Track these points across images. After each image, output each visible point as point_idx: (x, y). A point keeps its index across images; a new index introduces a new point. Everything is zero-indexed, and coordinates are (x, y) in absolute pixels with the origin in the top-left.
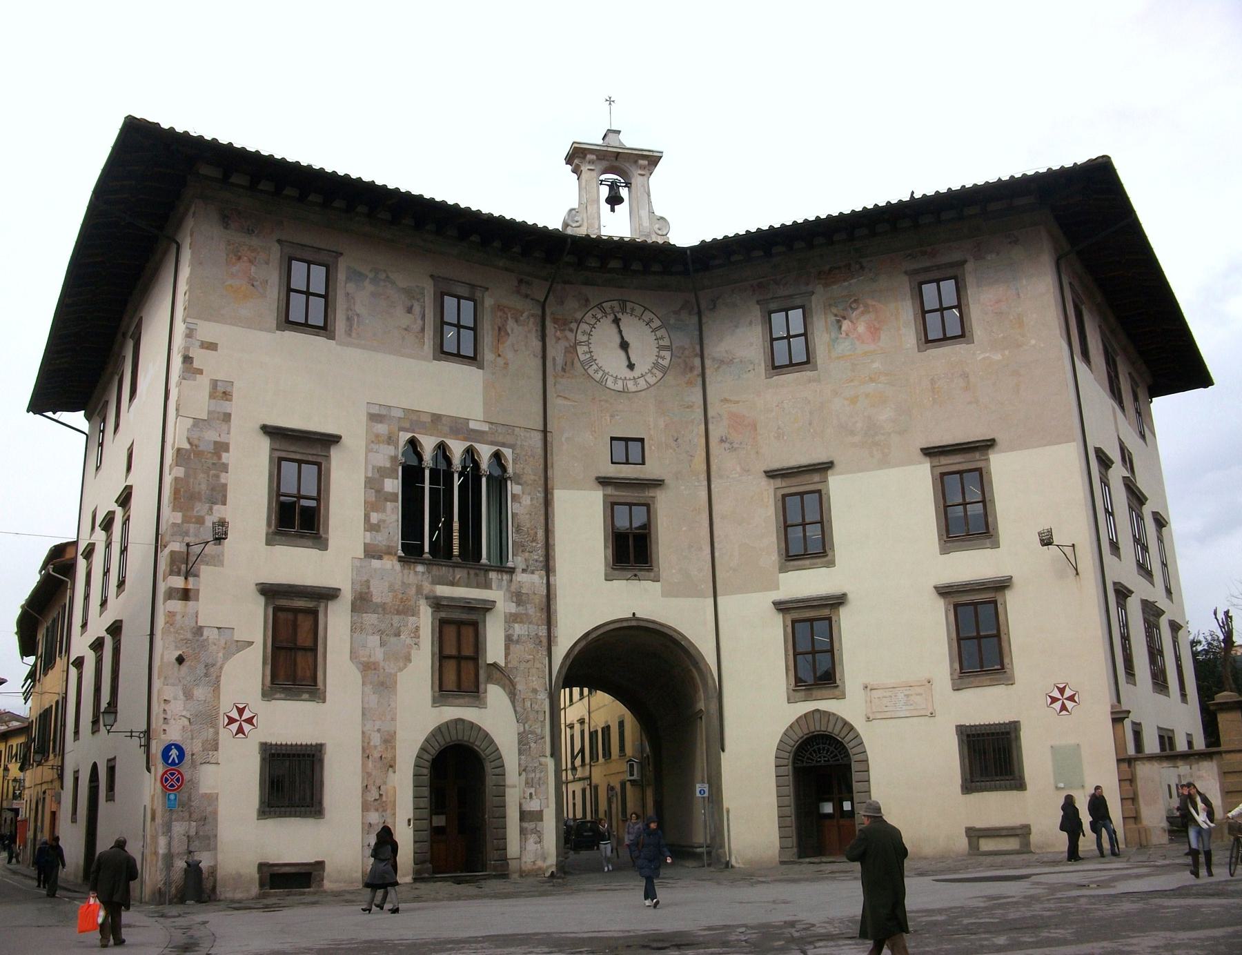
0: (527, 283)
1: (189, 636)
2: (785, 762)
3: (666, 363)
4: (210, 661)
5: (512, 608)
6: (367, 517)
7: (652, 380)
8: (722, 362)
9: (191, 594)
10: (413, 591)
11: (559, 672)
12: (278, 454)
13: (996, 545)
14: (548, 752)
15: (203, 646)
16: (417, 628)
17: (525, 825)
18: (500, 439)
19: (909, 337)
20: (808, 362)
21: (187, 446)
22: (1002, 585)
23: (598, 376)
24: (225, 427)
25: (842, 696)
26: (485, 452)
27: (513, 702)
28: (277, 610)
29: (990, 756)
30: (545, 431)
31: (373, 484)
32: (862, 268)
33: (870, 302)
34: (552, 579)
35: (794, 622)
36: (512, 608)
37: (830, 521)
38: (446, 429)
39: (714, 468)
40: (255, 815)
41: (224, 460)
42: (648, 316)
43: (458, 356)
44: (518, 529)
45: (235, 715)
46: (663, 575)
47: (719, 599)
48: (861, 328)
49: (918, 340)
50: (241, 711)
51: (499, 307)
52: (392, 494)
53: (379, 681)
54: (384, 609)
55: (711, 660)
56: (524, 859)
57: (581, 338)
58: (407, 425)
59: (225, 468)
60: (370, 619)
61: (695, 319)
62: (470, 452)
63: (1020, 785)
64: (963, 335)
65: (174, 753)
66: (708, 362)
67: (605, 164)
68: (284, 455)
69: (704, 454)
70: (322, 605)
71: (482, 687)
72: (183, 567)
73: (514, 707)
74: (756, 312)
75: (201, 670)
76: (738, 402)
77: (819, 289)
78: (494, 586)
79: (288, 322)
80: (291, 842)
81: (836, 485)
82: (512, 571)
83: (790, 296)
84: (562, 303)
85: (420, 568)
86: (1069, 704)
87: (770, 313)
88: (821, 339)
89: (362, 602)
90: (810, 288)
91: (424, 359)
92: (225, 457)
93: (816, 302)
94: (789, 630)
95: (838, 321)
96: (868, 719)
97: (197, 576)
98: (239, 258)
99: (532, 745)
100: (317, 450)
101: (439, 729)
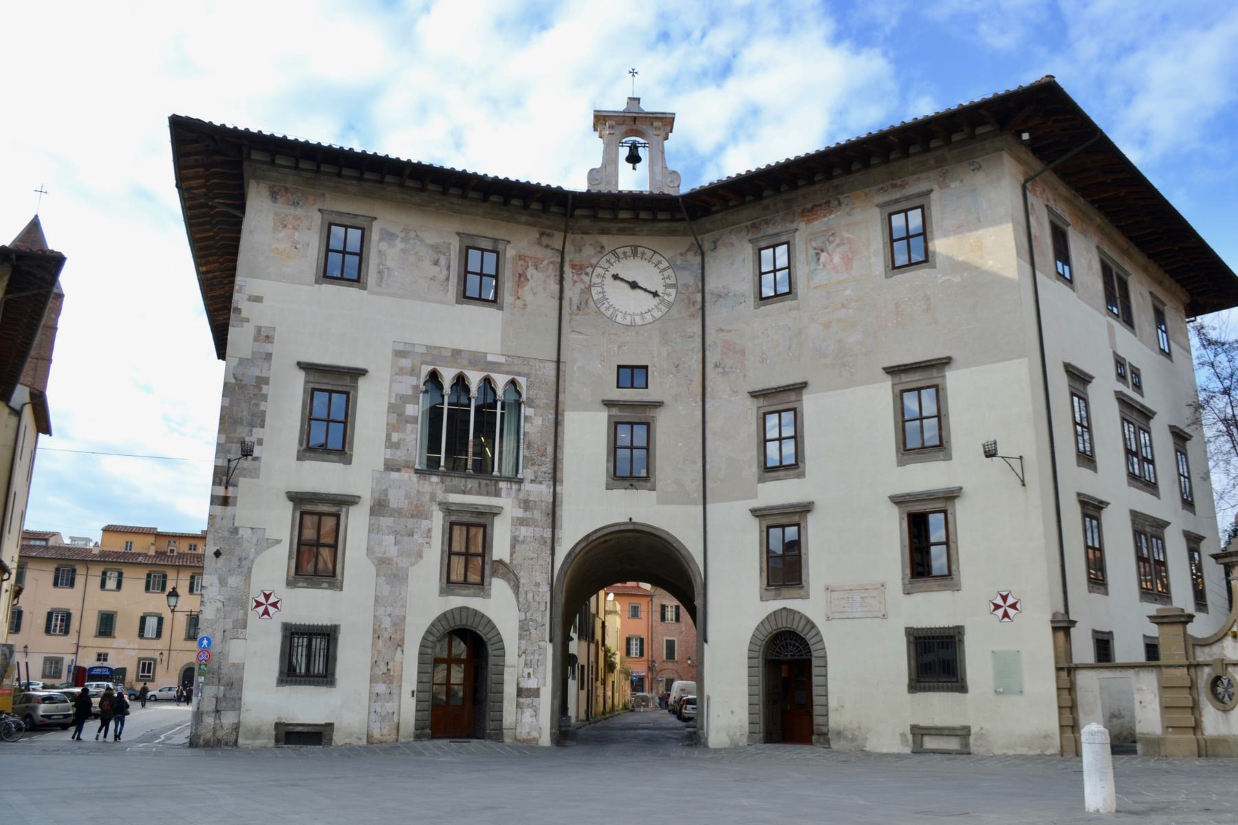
0: (548, 235)
1: (226, 534)
2: (756, 654)
3: (671, 299)
4: (243, 555)
5: (520, 513)
6: (388, 437)
7: (657, 314)
9: (230, 501)
10: (428, 497)
11: (562, 568)
12: (312, 385)
13: (948, 457)
14: (547, 638)
15: (239, 543)
16: (429, 530)
17: (522, 700)
18: (516, 369)
21: (233, 381)
23: (608, 313)
24: (266, 365)
25: (807, 597)
26: (500, 381)
27: (517, 593)
29: (936, 659)
30: (558, 362)
31: (395, 409)
33: (846, 235)
34: (558, 488)
35: (768, 527)
36: (520, 513)
37: (802, 436)
38: (465, 362)
39: (708, 389)
41: (264, 391)
42: (657, 257)
43: (480, 300)
44: (529, 446)
45: (262, 599)
46: (659, 485)
47: (708, 506)
48: (837, 259)
49: (886, 267)
50: (267, 597)
51: (521, 257)
52: (412, 417)
53: (391, 573)
54: (400, 513)
55: (699, 561)
56: (519, 730)
57: (595, 280)
58: (429, 359)
59: (264, 398)
60: (386, 521)
61: (698, 259)
62: (487, 381)
63: (963, 689)
66: (708, 298)
67: (624, 128)
68: (317, 386)
70: (344, 510)
71: (487, 580)
72: (224, 479)
73: (518, 598)
74: (749, 250)
75: (235, 562)
76: (730, 331)
77: (802, 226)
78: (503, 494)
80: (306, 705)
82: (521, 481)
83: (777, 234)
84: (580, 251)
85: (435, 479)
86: (1011, 612)
88: (801, 271)
89: (380, 507)
90: (795, 225)
92: (265, 389)
93: (799, 240)
94: (764, 535)
95: (817, 254)
96: (828, 619)
97: (235, 485)
98: (285, 226)
99: (533, 631)
100: (347, 381)
101: (444, 616)
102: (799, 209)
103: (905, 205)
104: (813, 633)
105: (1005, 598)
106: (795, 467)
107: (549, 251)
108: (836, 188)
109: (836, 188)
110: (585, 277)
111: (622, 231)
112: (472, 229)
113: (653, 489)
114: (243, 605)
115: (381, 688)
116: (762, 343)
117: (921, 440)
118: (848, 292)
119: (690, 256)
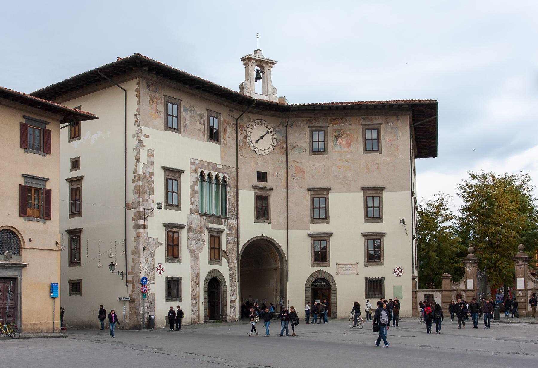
1: (146, 241)
3: (274, 145)
6: (191, 199)
7: (270, 151)
8: (294, 147)
12: (167, 177)
13: (382, 222)
18: (225, 171)
19: (360, 148)
20: (325, 152)
22: (383, 235)
23: (253, 149)
25: (329, 266)
26: (221, 175)
28: (168, 232)
30: (237, 168)
31: (192, 188)
32: (346, 120)
35: (314, 241)
38: (211, 168)
40: (164, 300)
45: (159, 268)
46: (272, 222)
48: (344, 142)
49: (363, 149)
51: (225, 121)
53: (195, 257)
59: (152, 182)
60: (192, 235)
61: (285, 129)
64: (378, 150)
65: (145, 280)
66: (289, 146)
69: (286, 180)
75: (149, 253)
77: (331, 125)
79: (168, 127)
81: (332, 196)
82: (228, 219)
84: (242, 119)
86: (400, 273)
87: (313, 131)
88: (330, 144)
90: (327, 125)
91: (205, 141)
93: (330, 130)
101: (211, 272)
102: (330, 118)
103: (371, 127)
104: (332, 279)
105: (398, 269)
106: (326, 219)
107: (232, 118)
108: (346, 113)
109: (346, 113)
110: (245, 132)
111: (257, 113)
112: (210, 108)
113: (270, 223)
114: (153, 270)
115: (194, 301)
116: (316, 171)
117: (374, 214)
118: (348, 156)
119: (281, 127)
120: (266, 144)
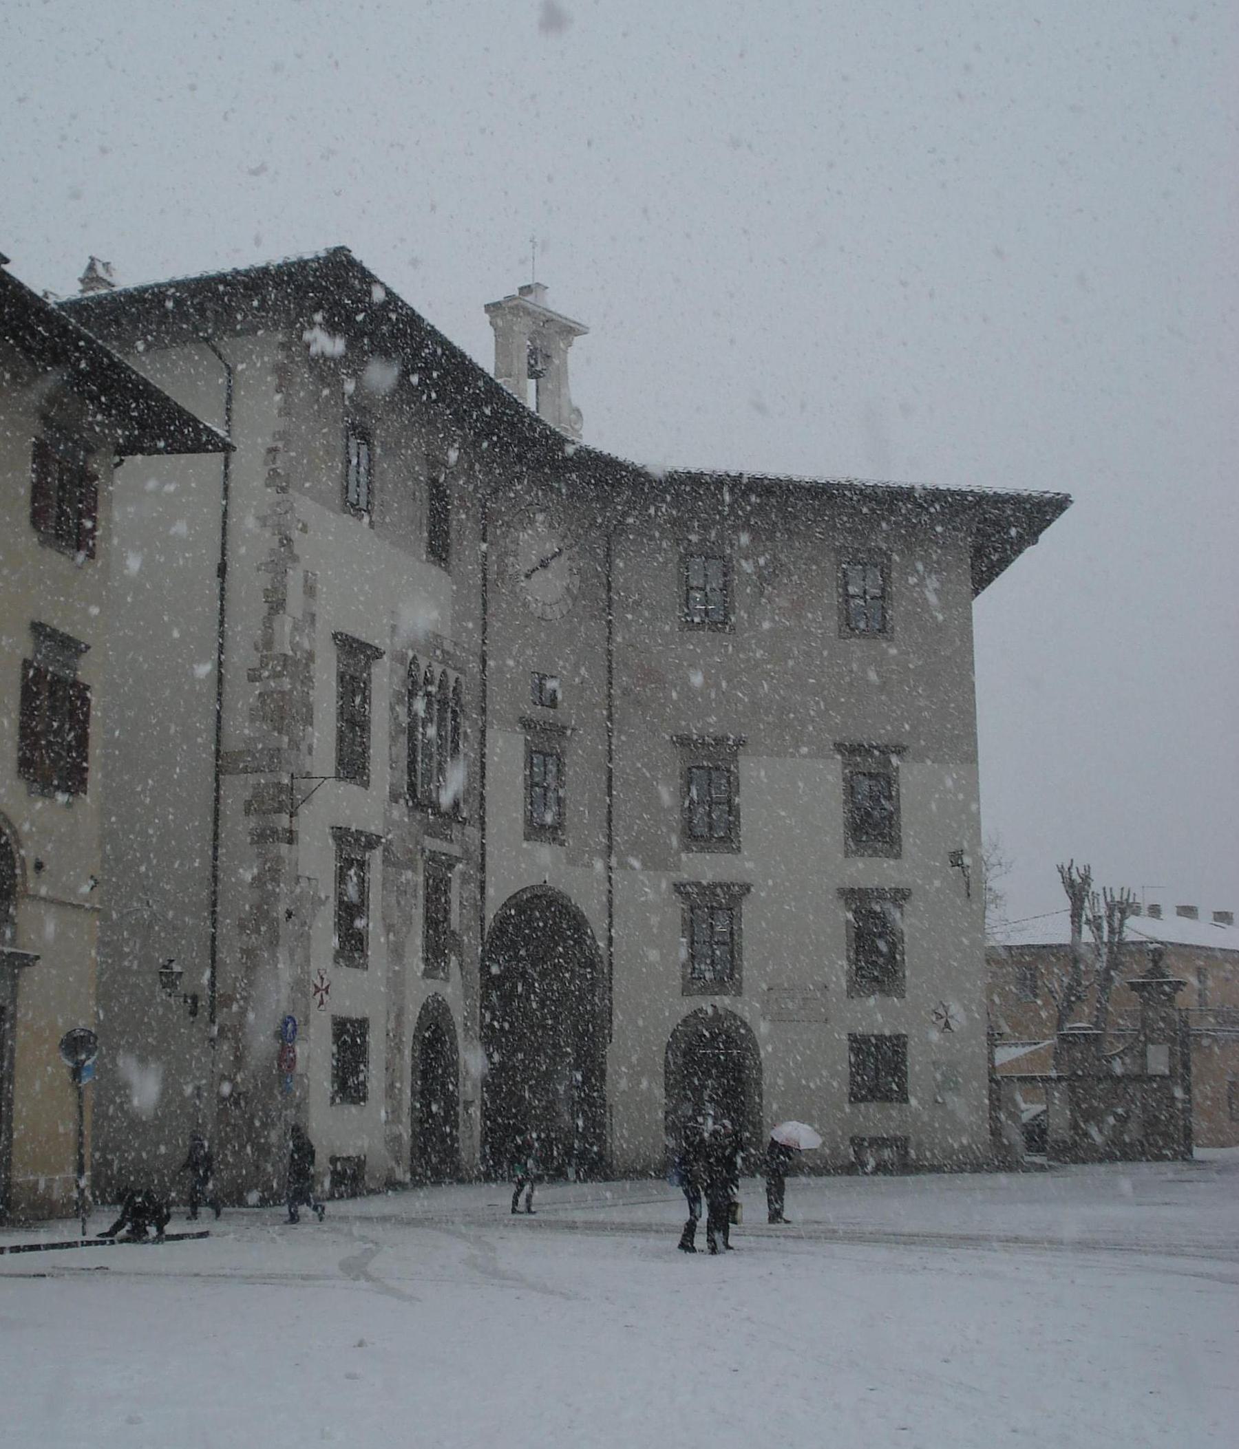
45: (318, 983)
120: (548, 590)
